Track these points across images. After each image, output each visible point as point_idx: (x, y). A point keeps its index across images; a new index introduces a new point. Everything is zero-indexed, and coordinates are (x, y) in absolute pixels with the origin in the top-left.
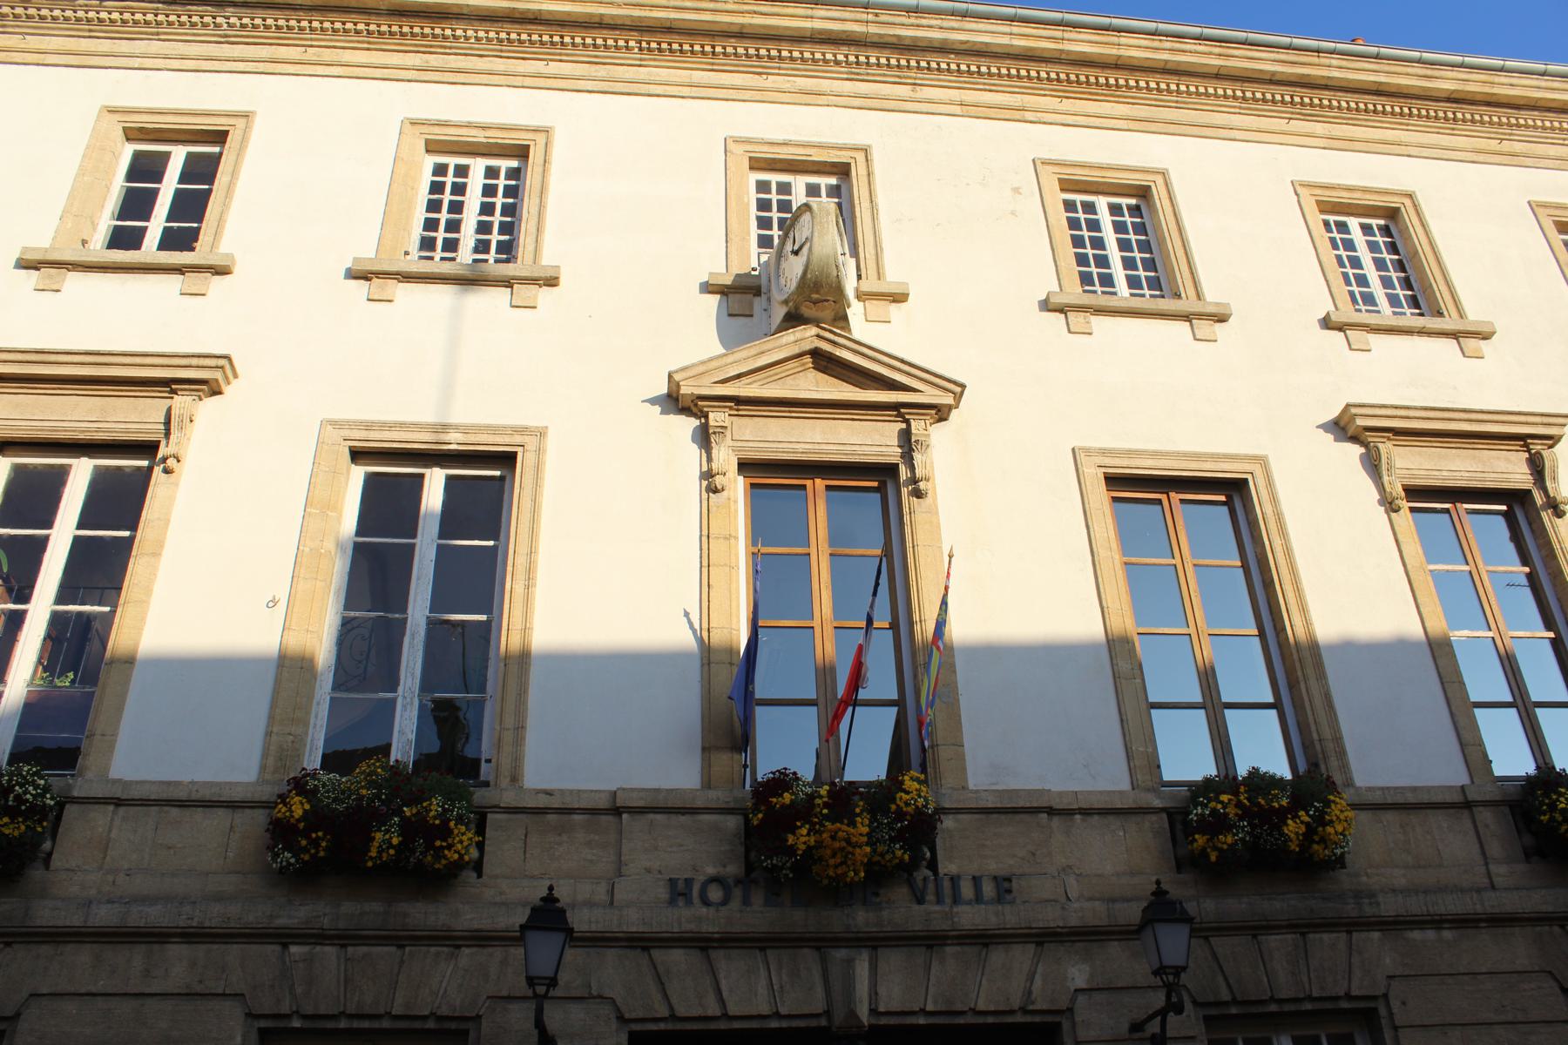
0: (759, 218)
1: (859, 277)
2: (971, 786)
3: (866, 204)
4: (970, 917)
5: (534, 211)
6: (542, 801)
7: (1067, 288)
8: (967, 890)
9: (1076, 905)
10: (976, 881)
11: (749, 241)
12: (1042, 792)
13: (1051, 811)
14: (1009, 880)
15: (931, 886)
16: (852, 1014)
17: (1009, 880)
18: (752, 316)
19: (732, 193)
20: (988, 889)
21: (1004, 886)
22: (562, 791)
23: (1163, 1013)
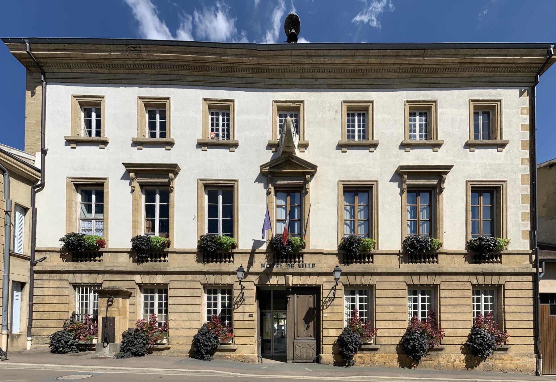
0: (280, 125)
1: (299, 139)
2: (310, 249)
3: (302, 119)
4: (308, 270)
5: (232, 125)
6: (242, 251)
7: (343, 140)
8: (307, 266)
9: (325, 268)
10: (309, 264)
11: (277, 131)
12: (322, 250)
13: (323, 253)
14: (314, 264)
15: (302, 265)
16: (289, 284)
17: (314, 264)
18: (277, 152)
19: (273, 118)
20: (311, 266)
21: (314, 265)
22: (245, 250)
23: (335, 286)
